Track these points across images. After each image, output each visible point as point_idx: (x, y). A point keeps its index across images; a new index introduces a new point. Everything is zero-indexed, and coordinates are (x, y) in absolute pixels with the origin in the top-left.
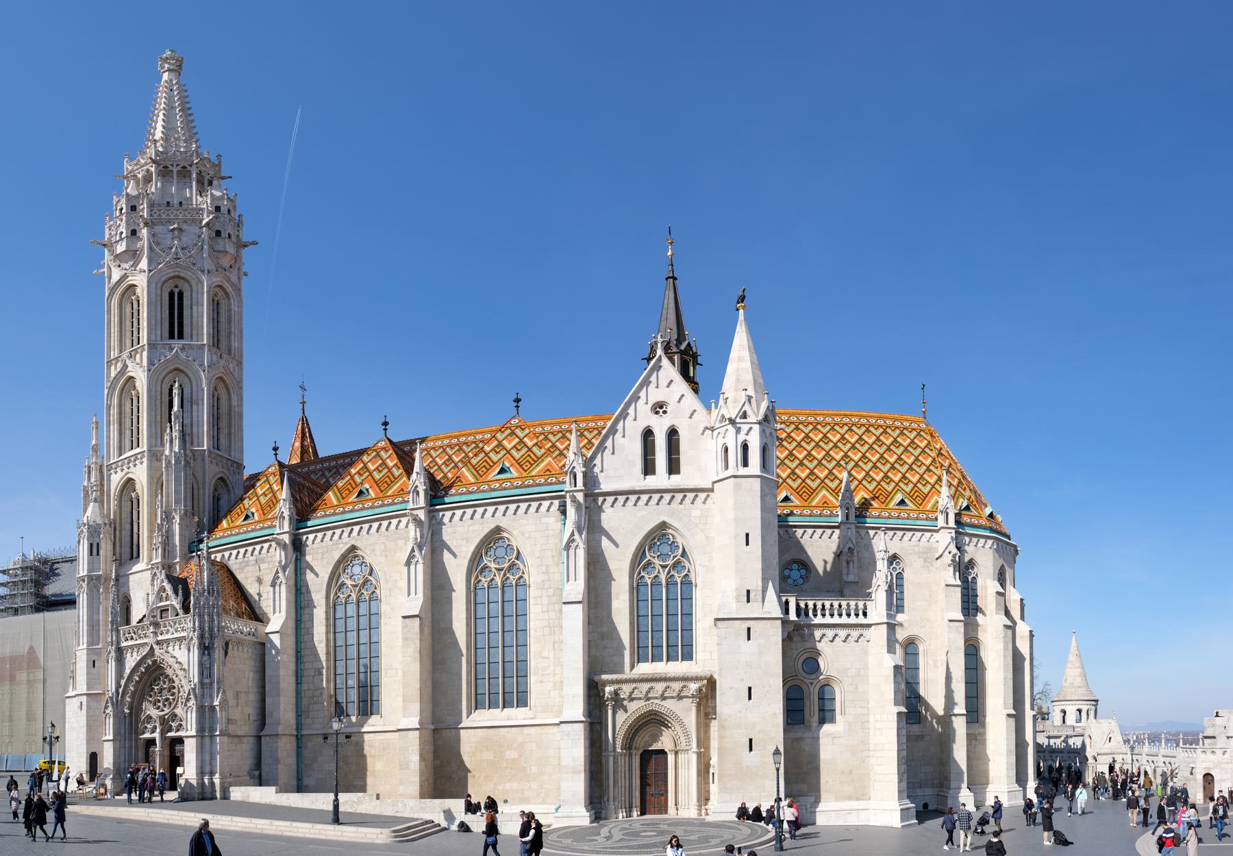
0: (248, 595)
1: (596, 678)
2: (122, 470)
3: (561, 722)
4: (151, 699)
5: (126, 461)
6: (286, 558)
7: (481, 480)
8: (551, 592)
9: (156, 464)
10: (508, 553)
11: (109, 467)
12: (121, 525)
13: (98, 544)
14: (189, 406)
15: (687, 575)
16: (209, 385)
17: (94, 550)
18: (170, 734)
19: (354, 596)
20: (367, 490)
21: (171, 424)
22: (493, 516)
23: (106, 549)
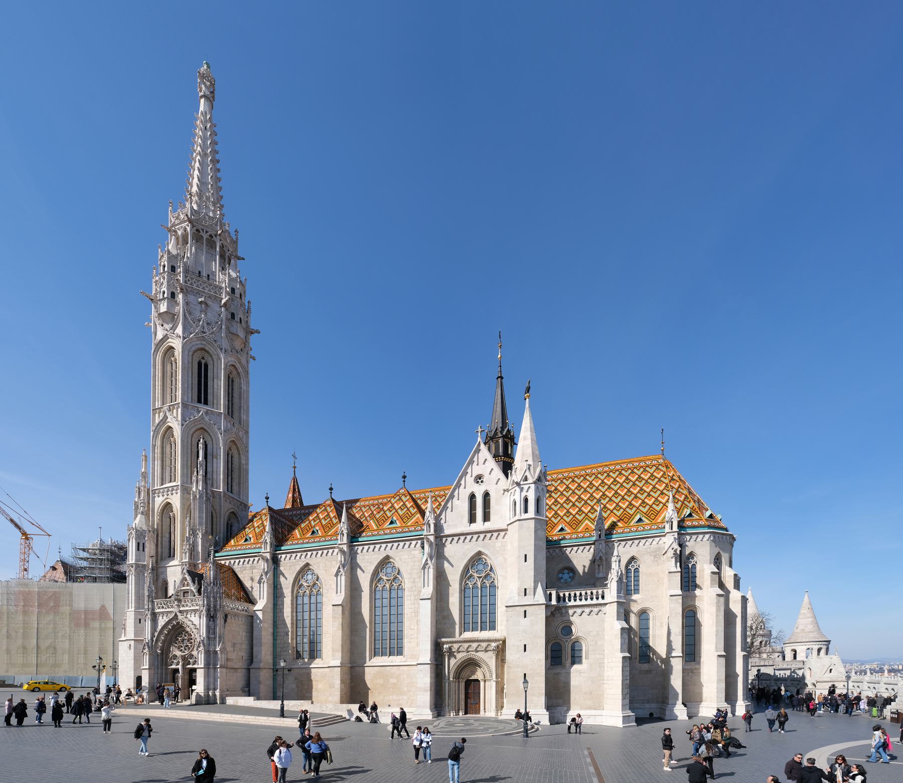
0: (245, 587)
1: (439, 640)
2: (163, 496)
3: (418, 664)
4: (176, 645)
5: (166, 490)
6: (268, 567)
7: (380, 528)
8: (416, 593)
9: (186, 495)
10: (393, 571)
11: (154, 492)
12: (162, 533)
13: (144, 544)
14: (211, 459)
15: (493, 581)
16: (224, 445)
17: (140, 547)
18: (188, 666)
19: (308, 592)
20: (317, 531)
21: (197, 469)
22: (385, 550)
23: (150, 548)
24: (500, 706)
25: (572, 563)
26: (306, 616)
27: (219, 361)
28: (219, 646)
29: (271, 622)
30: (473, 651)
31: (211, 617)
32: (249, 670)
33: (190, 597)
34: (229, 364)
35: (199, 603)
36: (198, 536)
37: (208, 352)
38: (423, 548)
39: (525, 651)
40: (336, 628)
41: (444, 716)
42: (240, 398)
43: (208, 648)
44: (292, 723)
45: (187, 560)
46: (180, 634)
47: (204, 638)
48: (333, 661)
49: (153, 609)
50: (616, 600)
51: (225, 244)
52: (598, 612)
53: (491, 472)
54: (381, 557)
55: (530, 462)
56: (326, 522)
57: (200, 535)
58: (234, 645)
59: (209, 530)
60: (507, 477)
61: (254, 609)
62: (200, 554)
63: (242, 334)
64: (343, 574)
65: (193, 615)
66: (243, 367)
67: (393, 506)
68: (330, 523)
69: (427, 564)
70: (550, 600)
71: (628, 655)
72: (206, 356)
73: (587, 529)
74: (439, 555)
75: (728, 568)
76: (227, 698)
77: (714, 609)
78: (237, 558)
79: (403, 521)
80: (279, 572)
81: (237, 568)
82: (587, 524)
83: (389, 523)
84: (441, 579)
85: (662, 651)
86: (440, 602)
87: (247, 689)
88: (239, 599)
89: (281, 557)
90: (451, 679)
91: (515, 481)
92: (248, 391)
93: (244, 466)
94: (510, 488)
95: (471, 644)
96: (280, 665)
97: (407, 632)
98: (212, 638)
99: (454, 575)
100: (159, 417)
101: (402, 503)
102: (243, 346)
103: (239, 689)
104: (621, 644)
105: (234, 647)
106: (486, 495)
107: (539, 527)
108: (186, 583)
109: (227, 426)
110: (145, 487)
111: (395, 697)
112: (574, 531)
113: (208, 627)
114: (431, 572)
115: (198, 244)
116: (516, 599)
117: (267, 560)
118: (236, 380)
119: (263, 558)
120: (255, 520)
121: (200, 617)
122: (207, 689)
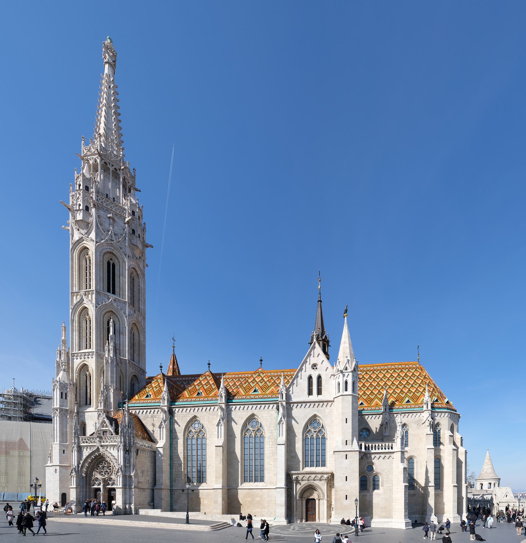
1: (290, 472)
2: (81, 358)
3: (276, 488)
4: (98, 471)
5: (83, 354)
9: (100, 360)
11: (73, 355)
13: (66, 394)
16: (129, 326)
17: (63, 396)
18: (108, 487)
24: (329, 516)
25: (369, 425)
26: (194, 453)
27: (124, 263)
28: (133, 472)
29: (168, 456)
30: (312, 480)
31: (127, 451)
32: (153, 490)
33: (108, 435)
34: (131, 267)
35: (118, 440)
36: (110, 391)
37: (115, 256)
38: (278, 409)
39: (346, 480)
40: (218, 462)
41: (293, 523)
42: (139, 293)
43: (125, 473)
44: (196, 528)
45: (102, 408)
46: (101, 462)
47: (121, 466)
48: (216, 485)
49: (79, 443)
50: (400, 450)
51: (126, 177)
52: (389, 457)
53: (322, 362)
54: (249, 415)
55: (349, 358)
56: (207, 387)
57: (112, 391)
58: (143, 472)
59: (119, 387)
60: (333, 367)
61: (157, 446)
62: (112, 404)
63: (140, 246)
64: (223, 425)
65: (112, 449)
66: (141, 270)
67: (254, 379)
68: (210, 388)
69: (282, 421)
70: (361, 448)
71: (407, 484)
72: (114, 258)
73: (377, 404)
74: (288, 415)
75: (457, 433)
76: (140, 510)
77: (451, 458)
78: (141, 409)
79: (263, 391)
80: (173, 421)
81: (141, 416)
82: (377, 402)
83: (253, 390)
84: (290, 432)
85: (422, 482)
86: (290, 447)
87: (152, 504)
88: (144, 438)
89: (175, 410)
90: (298, 498)
91: (340, 370)
92: (145, 289)
93: (143, 343)
94: (336, 374)
95: (311, 475)
96: (186, 487)
97: (266, 466)
98: (127, 466)
99: (298, 429)
100: (76, 298)
101: (261, 378)
102: (141, 255)
103: (147, 504)
104: (404, 478)
105: (143, 473)
106: (319, 378)
107: (354, 401)
108: (105, 425)
109: (130, 312)
110: (65, 351)
111: (259, 510)
112: (369, 405)
113: (125, 458)
114: (284, 426)
115: (106, 173)
116: (341, 447)
117: (165, 412)
118: (136, 279)
119: (162, 410)
120: (153, 382)
121: (118, 451)
122: (125, 503)
